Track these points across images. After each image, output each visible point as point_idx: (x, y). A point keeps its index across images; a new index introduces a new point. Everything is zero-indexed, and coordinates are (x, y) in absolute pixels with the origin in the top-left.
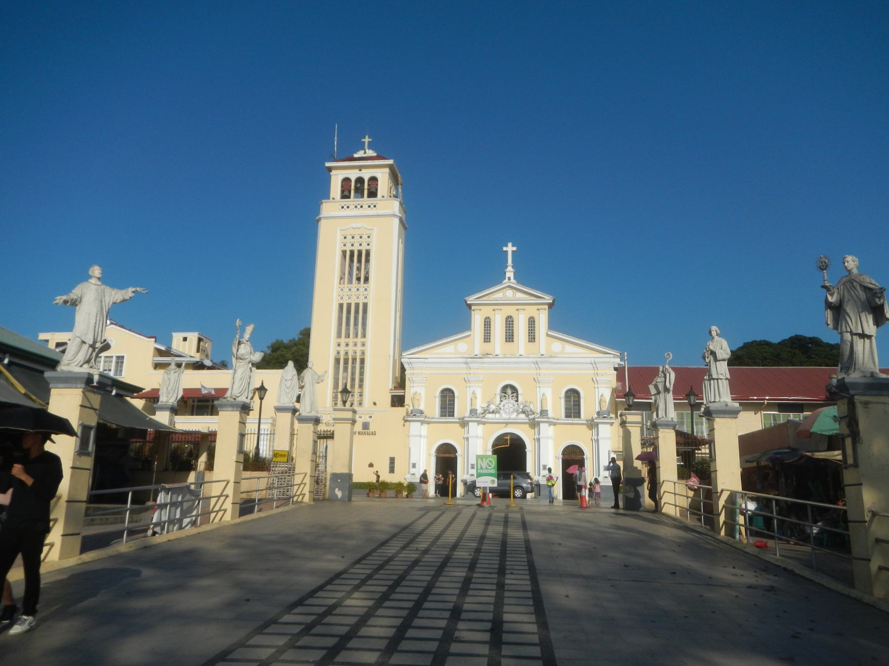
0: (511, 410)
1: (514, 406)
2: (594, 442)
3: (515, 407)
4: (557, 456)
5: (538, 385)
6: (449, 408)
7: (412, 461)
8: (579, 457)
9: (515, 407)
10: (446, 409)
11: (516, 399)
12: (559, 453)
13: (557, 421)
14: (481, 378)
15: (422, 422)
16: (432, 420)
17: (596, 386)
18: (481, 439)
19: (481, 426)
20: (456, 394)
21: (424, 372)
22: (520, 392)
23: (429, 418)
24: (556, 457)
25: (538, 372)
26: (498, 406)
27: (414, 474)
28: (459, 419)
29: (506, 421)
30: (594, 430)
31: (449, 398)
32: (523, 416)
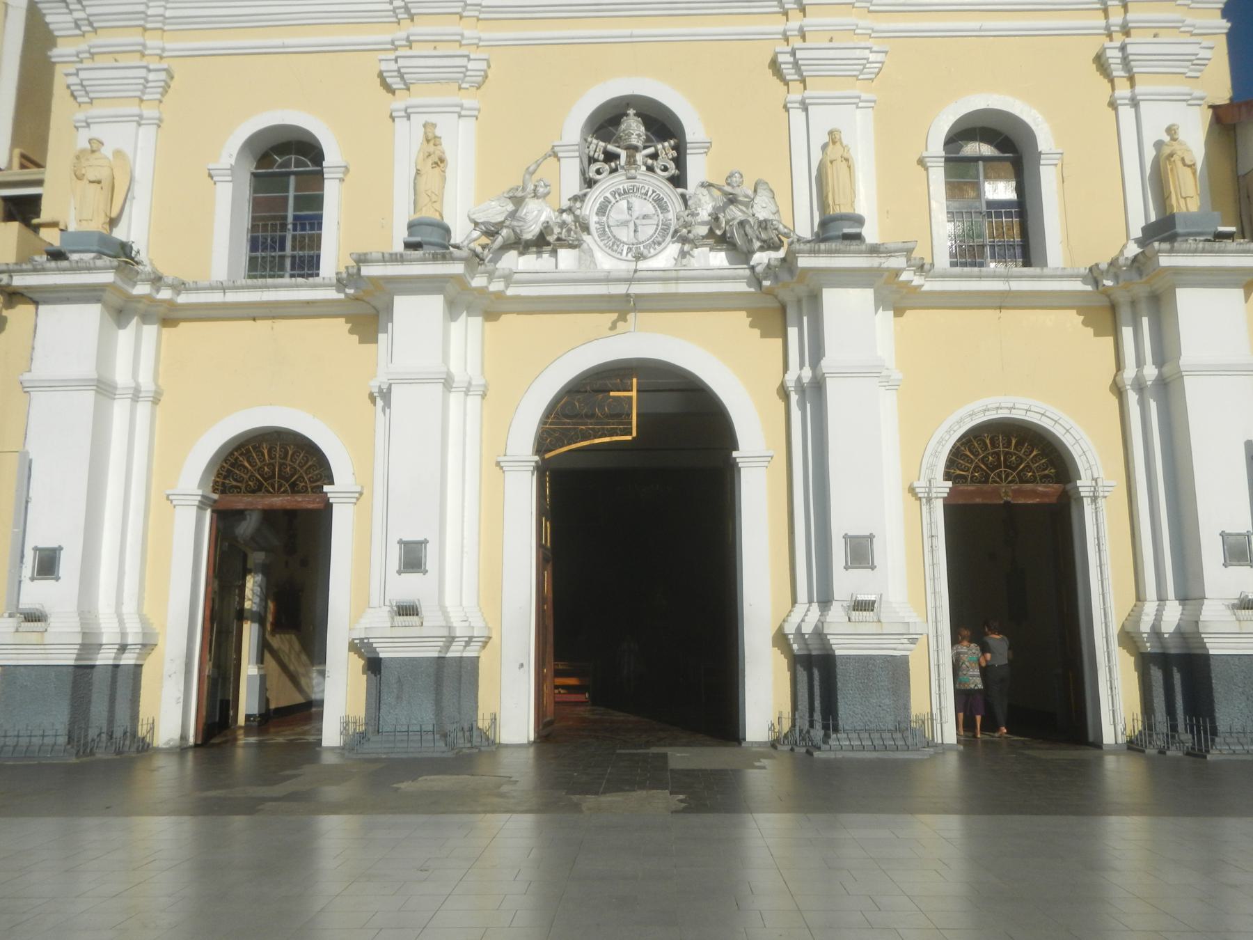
0: (647, 231)
1: (664, 209)
2: (1132, 398)
3: (671, 215)
4: (920, 484)
5: (795, 95)
6: (299, 243)
7: (39, 536)
8: (1041, 488)
9: (671, 215)
10: (282, 248)
11: (673, 170)
12: (932, 468)
13: (917, 280)
14: (471, 65)
15: (121, 311)
16: (183, 299)
17: (1123, 91)
18: (474, 402)
19: (469, 328)
20: (332, 158)
21: (153, 42)
22: (694, 130)
23: (157, 280)
24: (912, 490)
25: (795, 23)
26: (570, 210)
27: (34, 617)
28: (341, 284)
29: (620, 289)
30: (1127, 333)
31: (296, 190)
32: (719, 259)
